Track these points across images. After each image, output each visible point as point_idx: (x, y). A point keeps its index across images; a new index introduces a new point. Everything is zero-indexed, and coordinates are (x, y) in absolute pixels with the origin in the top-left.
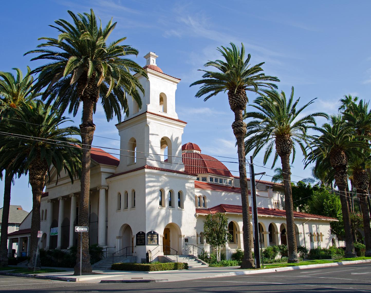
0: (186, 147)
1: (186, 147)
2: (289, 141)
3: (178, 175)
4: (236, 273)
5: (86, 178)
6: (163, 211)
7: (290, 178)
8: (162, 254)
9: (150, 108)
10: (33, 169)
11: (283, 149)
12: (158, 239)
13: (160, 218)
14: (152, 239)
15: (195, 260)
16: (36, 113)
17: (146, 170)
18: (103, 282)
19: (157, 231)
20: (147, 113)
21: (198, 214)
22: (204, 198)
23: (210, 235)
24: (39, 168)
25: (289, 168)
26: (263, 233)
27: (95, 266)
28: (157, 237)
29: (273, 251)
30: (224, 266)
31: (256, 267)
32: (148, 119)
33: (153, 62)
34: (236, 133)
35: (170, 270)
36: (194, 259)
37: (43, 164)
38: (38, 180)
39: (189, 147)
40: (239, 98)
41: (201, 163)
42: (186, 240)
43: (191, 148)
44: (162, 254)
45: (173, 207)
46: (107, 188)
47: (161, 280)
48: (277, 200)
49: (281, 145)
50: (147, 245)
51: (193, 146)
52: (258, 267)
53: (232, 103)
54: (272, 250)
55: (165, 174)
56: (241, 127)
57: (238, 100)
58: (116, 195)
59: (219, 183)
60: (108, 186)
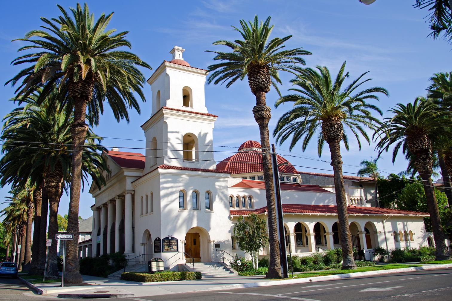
0: (245, 145)
1: (245, 145)
2: (338, 124)
3: (204, 173)
4: (244, 286)
5: (75, 181)
6: (185, 214)
7: (341, 168)
8: (182, 261)
9: (170, 104)
10: (48, 177)
11: (329, 134)
12: (177, 245)
13: (180, 221)
14: (169, 246)
15: (224, 268)
16: (48, 120)
17: (160, 170)
18: (60, 296)
19: (175, 236)
20: (163, 109)
21: (232, 216)
22: (250, 198)
23: (242, 239)
24: (53, 175)
25: (339, 157)
26: (325, 234)
27: (114, 276)
28: (176, 243)
29: (336, 255)
30: (257, 275)
31: (282, 277)
32: (165, 116)
33: (179, 56)
34: (257, 119)
35: (175, 280)
36: (223, 267)
37: (57, 171)
38: (52, 187)
39: (248, 145)
40: (259, 79)
41: (257, 161)
42: (217, 245)
43: (250, 146)
44: (182, 261)
45: (198, 210)
46: (133, 193)
47: (125, 295)
48: (359, 195)
49: (327, 130)
50: (163, 252)
51: (252, 144)
52: (286, 277)
53: (251, 86)
54: (334, 254)
55: (187, 174)
56: (262, 112)
57: (258, 81)
58: (140, 199)
59: (292, 182)
60: (134, 191)
